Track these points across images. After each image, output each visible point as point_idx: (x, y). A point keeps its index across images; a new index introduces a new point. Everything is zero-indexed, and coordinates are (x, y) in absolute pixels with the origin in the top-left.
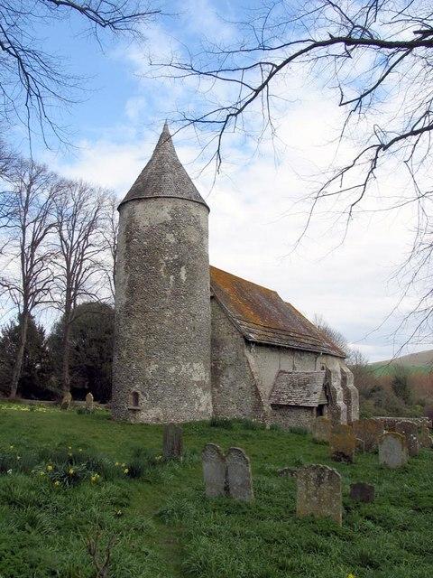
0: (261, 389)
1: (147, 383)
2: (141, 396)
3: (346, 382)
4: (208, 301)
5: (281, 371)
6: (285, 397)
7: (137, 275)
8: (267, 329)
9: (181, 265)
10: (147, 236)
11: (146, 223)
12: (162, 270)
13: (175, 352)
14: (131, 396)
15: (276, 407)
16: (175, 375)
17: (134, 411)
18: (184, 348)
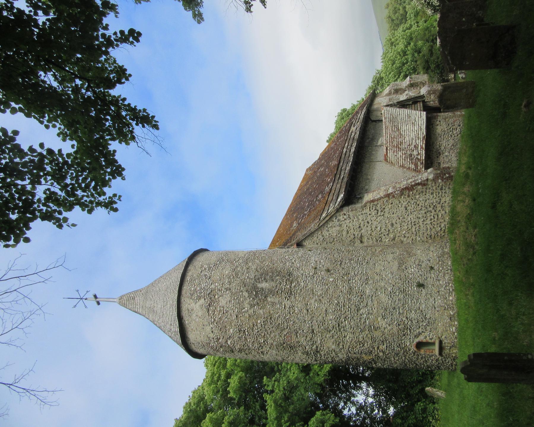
0: (403, 184)
1: (405, 330)
2: (421, 338)
3: (400, 89)
4: (301, 251)
5: (386, 160)
6: (415, 153)
7: (270, 341)
8: (337, 178)
9: (255, 288)
10: (223, 329)
11: (208, 329)
12: (261, 311)
13: (362, 295)
14: (422, 352)
15: (427, 166)
16: (391, 294)
17: (441, 349)
18: (356, 283)
